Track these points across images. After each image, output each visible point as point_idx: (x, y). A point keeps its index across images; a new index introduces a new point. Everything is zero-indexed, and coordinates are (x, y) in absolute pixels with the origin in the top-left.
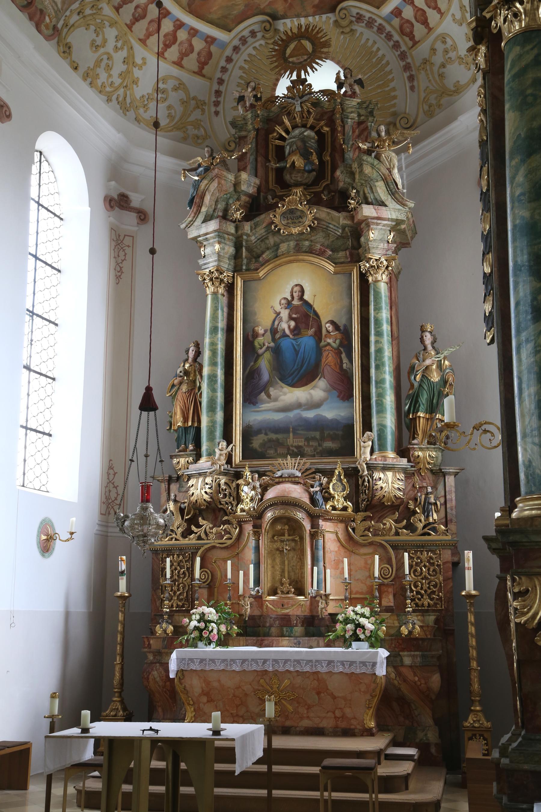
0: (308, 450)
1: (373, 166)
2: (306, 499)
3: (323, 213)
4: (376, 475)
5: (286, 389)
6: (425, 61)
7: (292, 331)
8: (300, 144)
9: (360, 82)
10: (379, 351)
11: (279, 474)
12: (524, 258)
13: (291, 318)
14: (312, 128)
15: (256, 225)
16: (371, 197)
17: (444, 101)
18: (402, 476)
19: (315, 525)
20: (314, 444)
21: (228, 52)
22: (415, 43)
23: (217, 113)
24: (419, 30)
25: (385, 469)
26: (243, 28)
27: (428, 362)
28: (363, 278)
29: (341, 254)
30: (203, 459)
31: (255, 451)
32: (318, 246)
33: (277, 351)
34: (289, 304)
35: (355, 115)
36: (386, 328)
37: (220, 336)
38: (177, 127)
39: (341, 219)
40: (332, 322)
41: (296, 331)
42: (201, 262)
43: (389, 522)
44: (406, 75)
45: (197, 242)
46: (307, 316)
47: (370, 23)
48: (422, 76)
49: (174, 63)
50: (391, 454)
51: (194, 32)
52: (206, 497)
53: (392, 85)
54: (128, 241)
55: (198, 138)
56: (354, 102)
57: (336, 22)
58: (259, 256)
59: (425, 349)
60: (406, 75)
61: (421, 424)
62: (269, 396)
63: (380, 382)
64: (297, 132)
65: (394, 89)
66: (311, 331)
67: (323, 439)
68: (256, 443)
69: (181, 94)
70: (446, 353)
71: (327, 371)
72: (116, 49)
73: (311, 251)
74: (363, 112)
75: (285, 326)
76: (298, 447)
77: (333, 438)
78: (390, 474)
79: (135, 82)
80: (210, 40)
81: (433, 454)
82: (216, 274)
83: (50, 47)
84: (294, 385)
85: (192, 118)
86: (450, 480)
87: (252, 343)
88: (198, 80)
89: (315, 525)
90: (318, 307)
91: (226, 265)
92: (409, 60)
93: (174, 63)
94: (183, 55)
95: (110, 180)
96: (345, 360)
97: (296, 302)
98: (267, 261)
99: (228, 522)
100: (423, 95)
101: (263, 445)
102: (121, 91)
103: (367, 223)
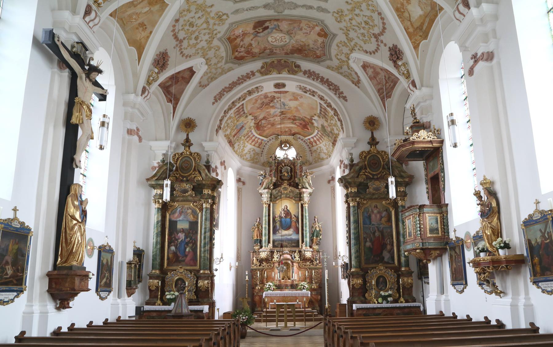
0: (288, 246)
1: (305, 179)
2: (291, 258)
3: (293, 189)
4: (306, 252)
5: (283, 231)
6: (315, 151)
7: (284, 217)
8: (286, 170)
9: (301, 157)
10: (306, 223)
11: (284, 252)
12: (353, 237)
13: (284, 213)
14: (289, 166)
15: (276, 190)
16: (304, 186)
17: (319, 160)
18: (311, 253)
19: (293, 264)
20: (290, 244)
21: (266, 142)
22: (313, 146)
23: (261, 156)
24: (314, 144)
25: (307, 251)
26: (271, 138)
27: (316, 225)
28: (302, 205)
29: (297, 199)
30: (263, 248)
31: (275, 245)
32: (291, 196)
33: (281, 221)
34: (284, 210)
35: (300, 164)
36: (307, 218)
37: (267, 217)
38: (252, 160)
39: (297, 191)
40: (294, 215)
41: (286, 217)
42: (262, 199)
43: (308, 263)
44: (310, 152)
45: (261, 194)
46: (288, 213)
47: (302, 140)
48: (314, 153)
49: (254, 145)
50: (308, 247)
51: (259, 139)
52: (265, 257)
53: (306, 153)
54: (240, 190)
55: (256, 162)
56: (300, 161)
57: (293, 138)
58: (276, 198)
59: (315, 222)
60: (310, 152)
61: (315, 240)
62: (279, 232)
63: (306, 231)
64: (286, 167)
65: (307, 154)
66: (289, 217)
67: (292, 243)
68: (276, 244)
69: (254, 152)
70: (320, 223)
71: (293, 227)
72: (242, 144)
73: (289, 197)
74: (301, 163)
75: (283, 215)
76: (286, 245)
77: (294, 243)
78: (308, 252)
79: (244, 151)
80: (262, 140)
81: (317, 247)
82: (266, 202)
83: (231, 148)
84: (285, 230)
85: (256, 157)
86: (321, 253)
87: (275, 219)
88: (258, 149)
89: (293, 264)
90: (291, 211)
91: (269, 199)
92: (311, 149)
93: (254, 145)
94: (256, 143)
95: (237, 175)
96: (297, 225)
97: (285, 210)
98: (279, 199)
99: (270, 263)
100: (314, 158)
101: (278, 244)
102: (241, 153)
103: (304, 193)
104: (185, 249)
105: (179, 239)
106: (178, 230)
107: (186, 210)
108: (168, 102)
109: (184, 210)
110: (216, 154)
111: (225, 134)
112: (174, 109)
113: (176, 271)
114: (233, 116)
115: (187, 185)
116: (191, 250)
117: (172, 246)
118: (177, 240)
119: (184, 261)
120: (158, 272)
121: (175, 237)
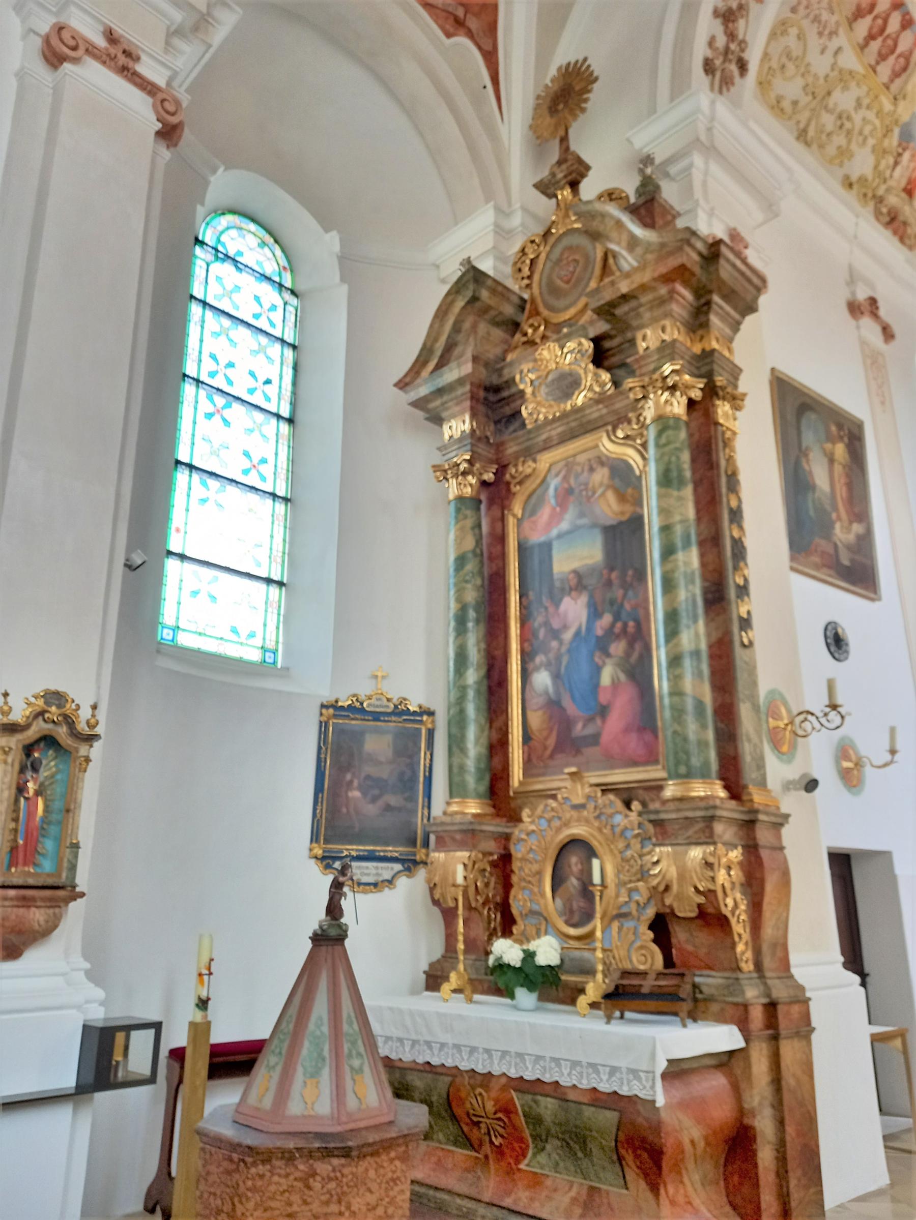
104: (598, 670)
105: (565, 627)
106: (557, 584)
107: (586, 474)
108: (449, 35)
109: (577, 476)
110: (715, 168)
111: (847, 177)
112: (491, 57)
113: (554, 797)
114: (859, 69)
115: (562, 348)
116: (622, 677)
117: (537, 669)
118: (555, 634)
119: (594, 740)
120: (473, 808)
121: (547, 624)
